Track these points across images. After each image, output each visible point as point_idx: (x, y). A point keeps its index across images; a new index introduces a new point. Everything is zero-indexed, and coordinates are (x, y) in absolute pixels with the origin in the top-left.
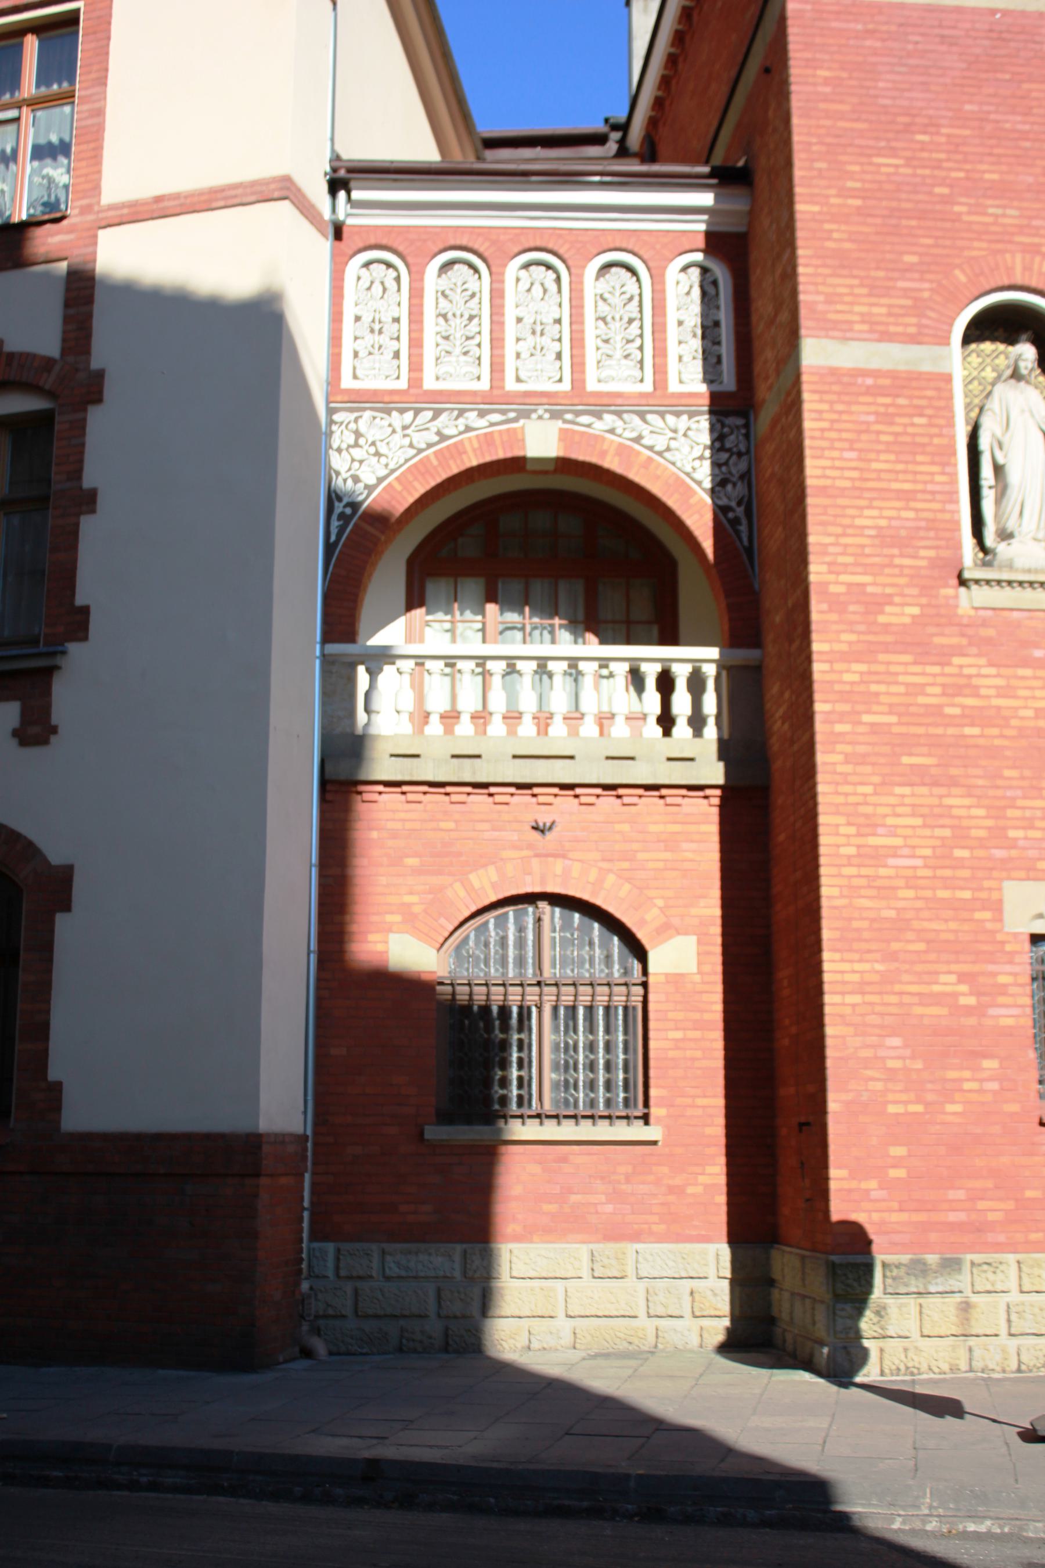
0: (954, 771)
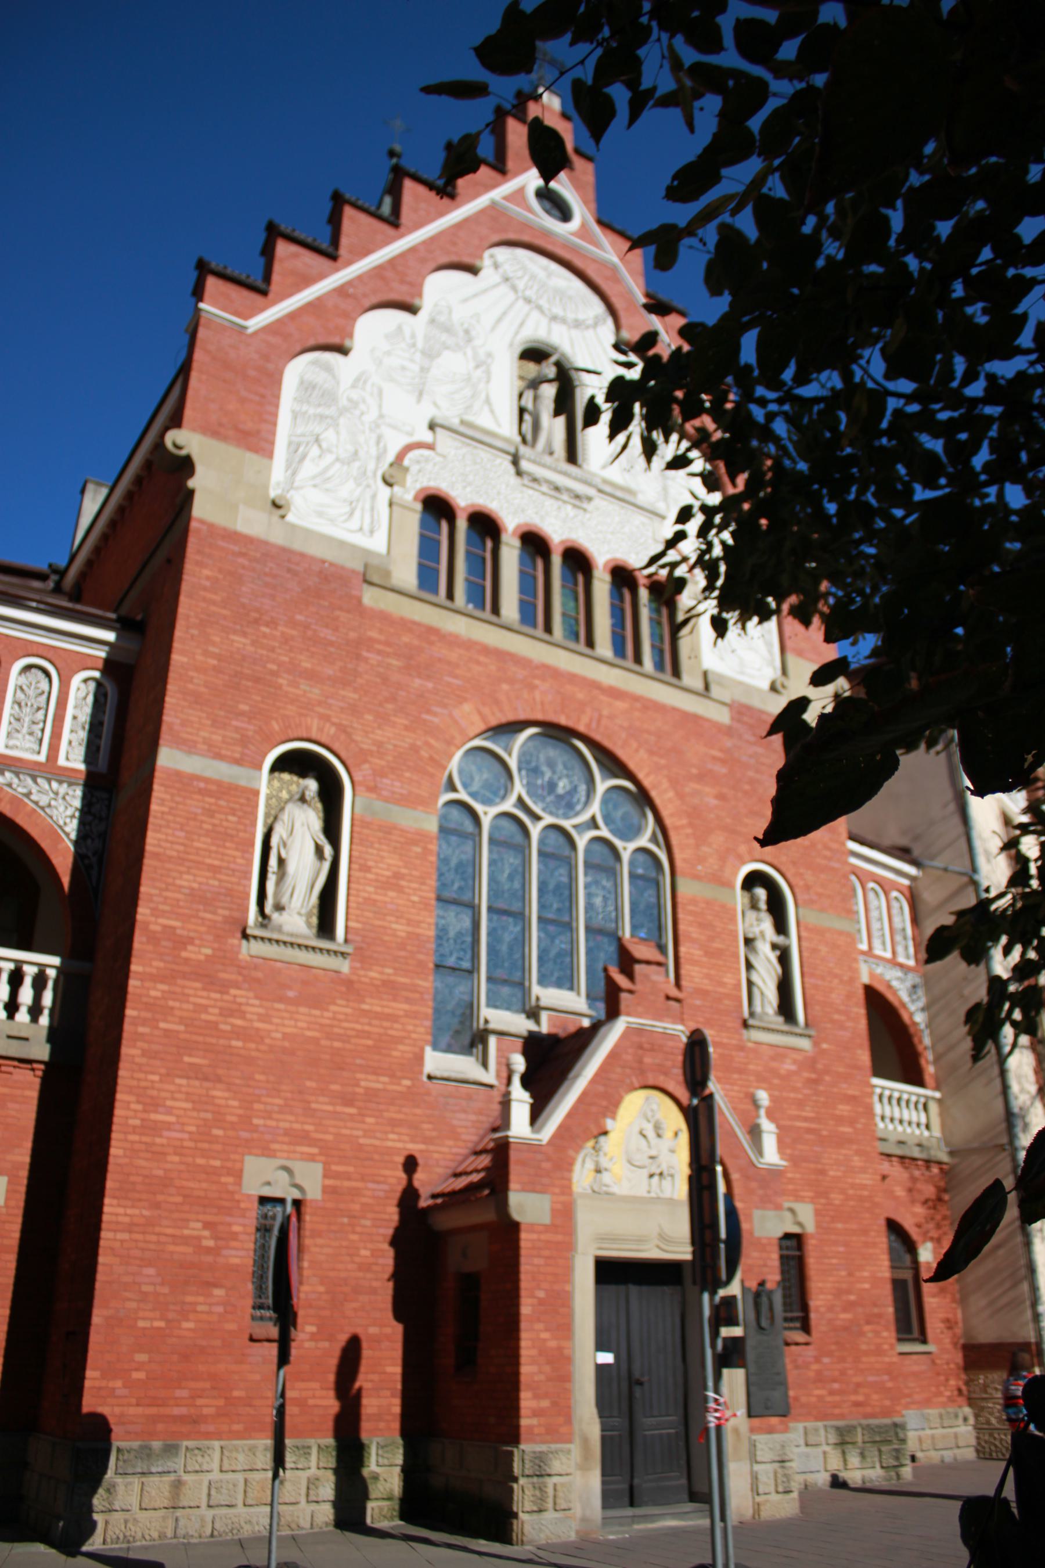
0: (220, 1072)
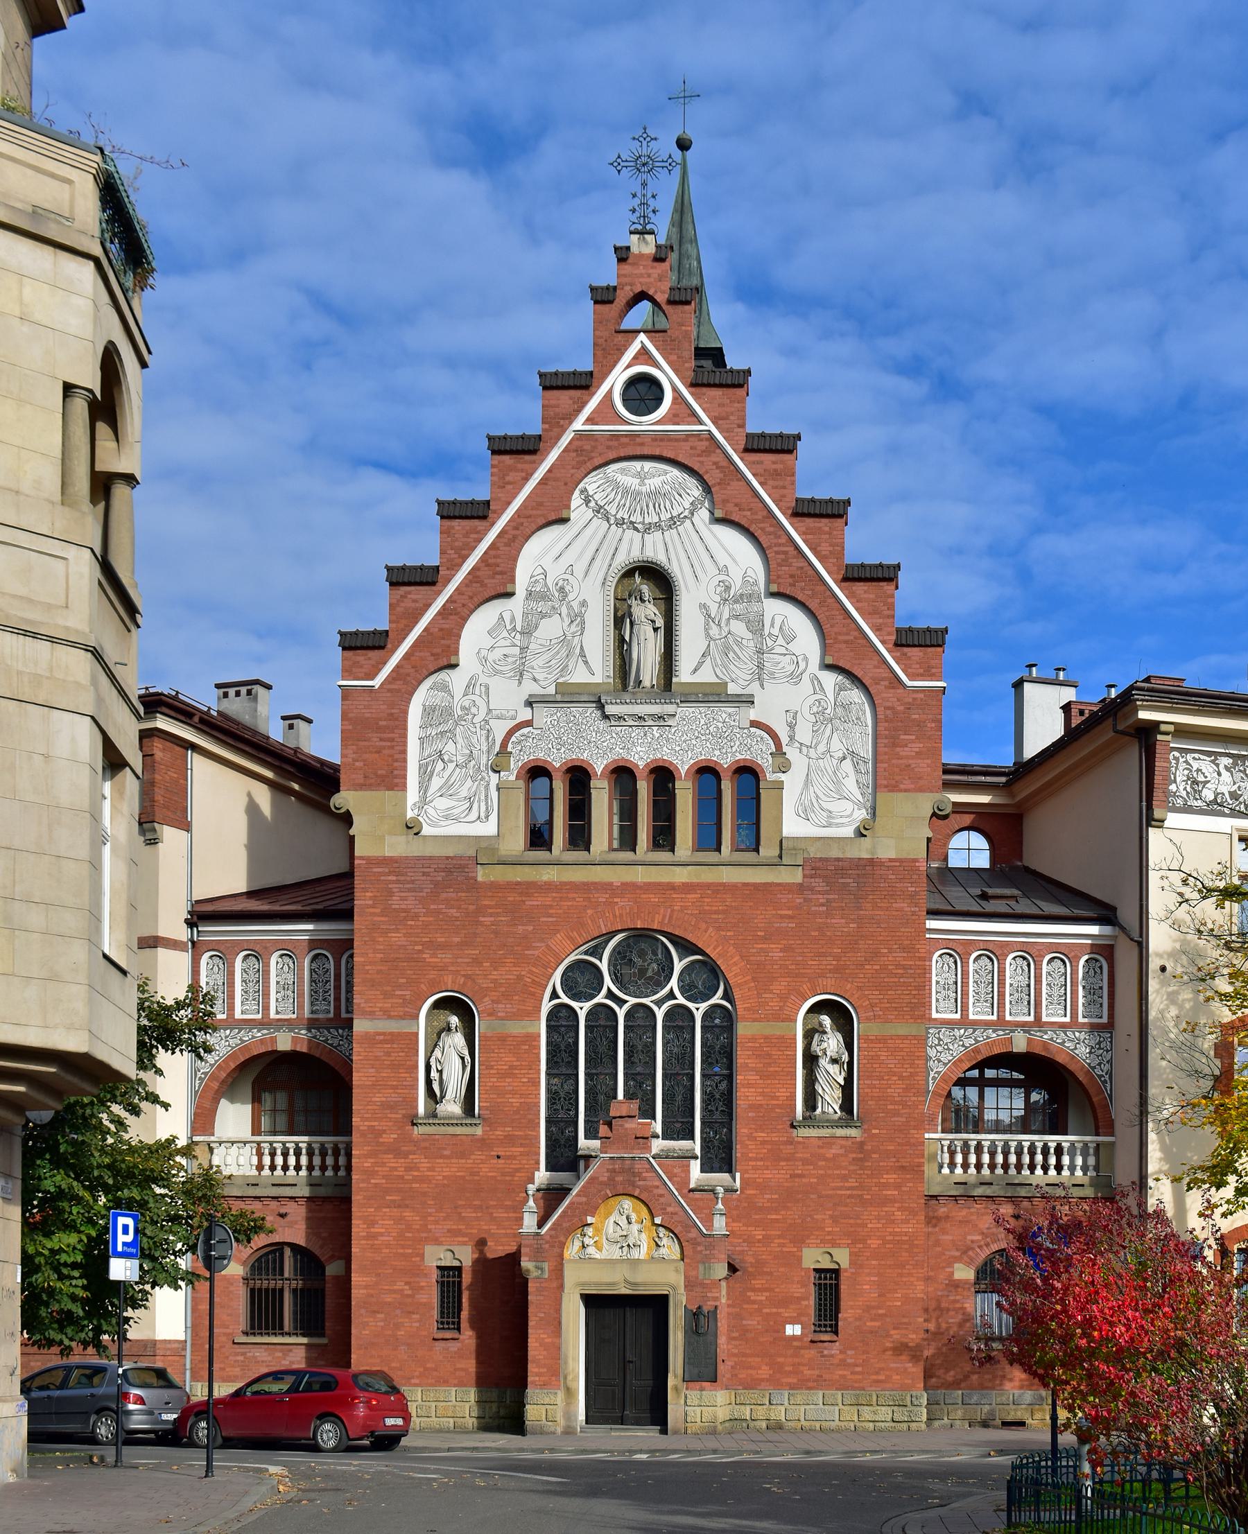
0: (407, 1202)
